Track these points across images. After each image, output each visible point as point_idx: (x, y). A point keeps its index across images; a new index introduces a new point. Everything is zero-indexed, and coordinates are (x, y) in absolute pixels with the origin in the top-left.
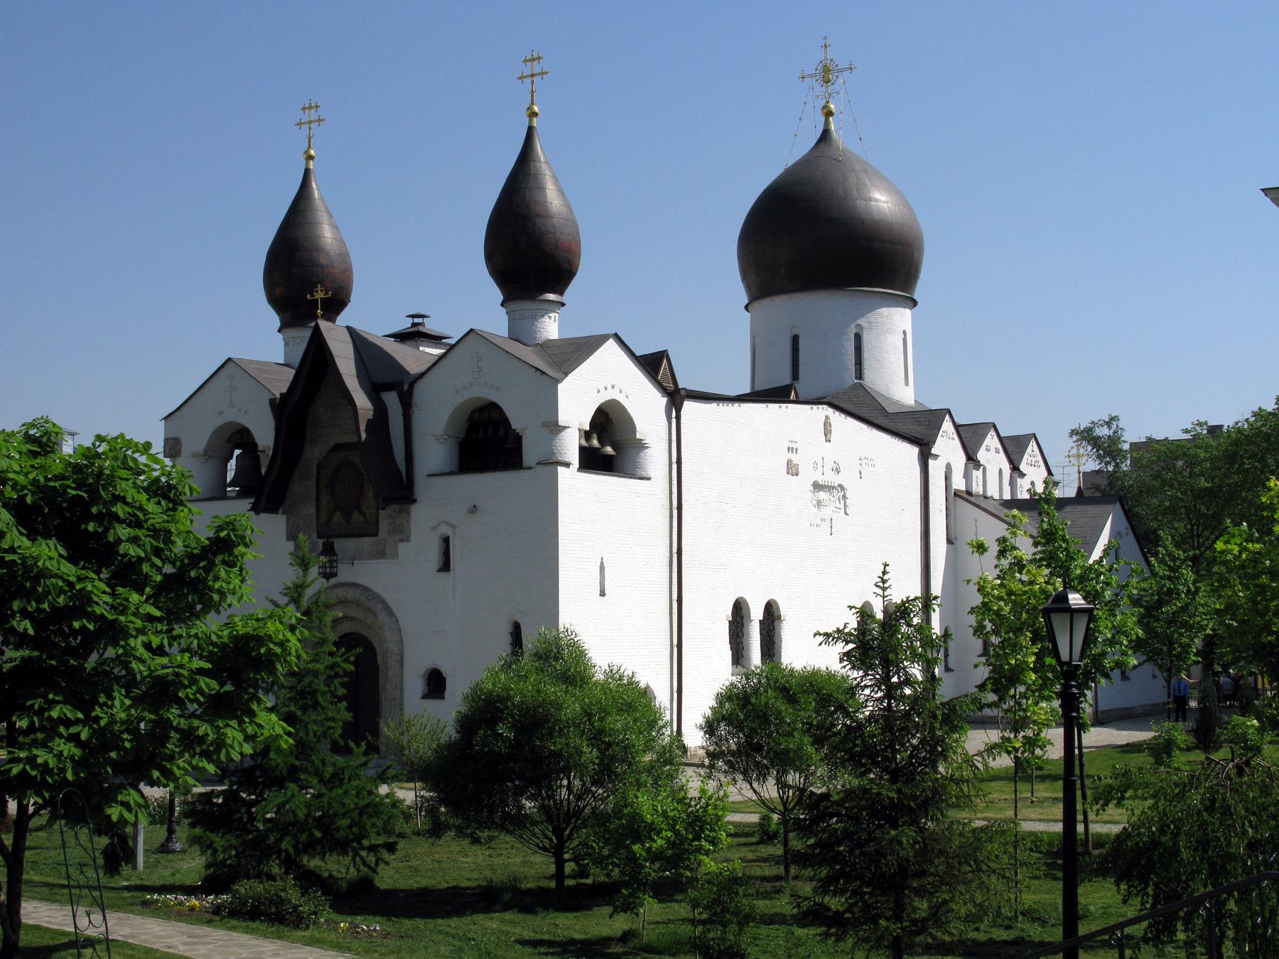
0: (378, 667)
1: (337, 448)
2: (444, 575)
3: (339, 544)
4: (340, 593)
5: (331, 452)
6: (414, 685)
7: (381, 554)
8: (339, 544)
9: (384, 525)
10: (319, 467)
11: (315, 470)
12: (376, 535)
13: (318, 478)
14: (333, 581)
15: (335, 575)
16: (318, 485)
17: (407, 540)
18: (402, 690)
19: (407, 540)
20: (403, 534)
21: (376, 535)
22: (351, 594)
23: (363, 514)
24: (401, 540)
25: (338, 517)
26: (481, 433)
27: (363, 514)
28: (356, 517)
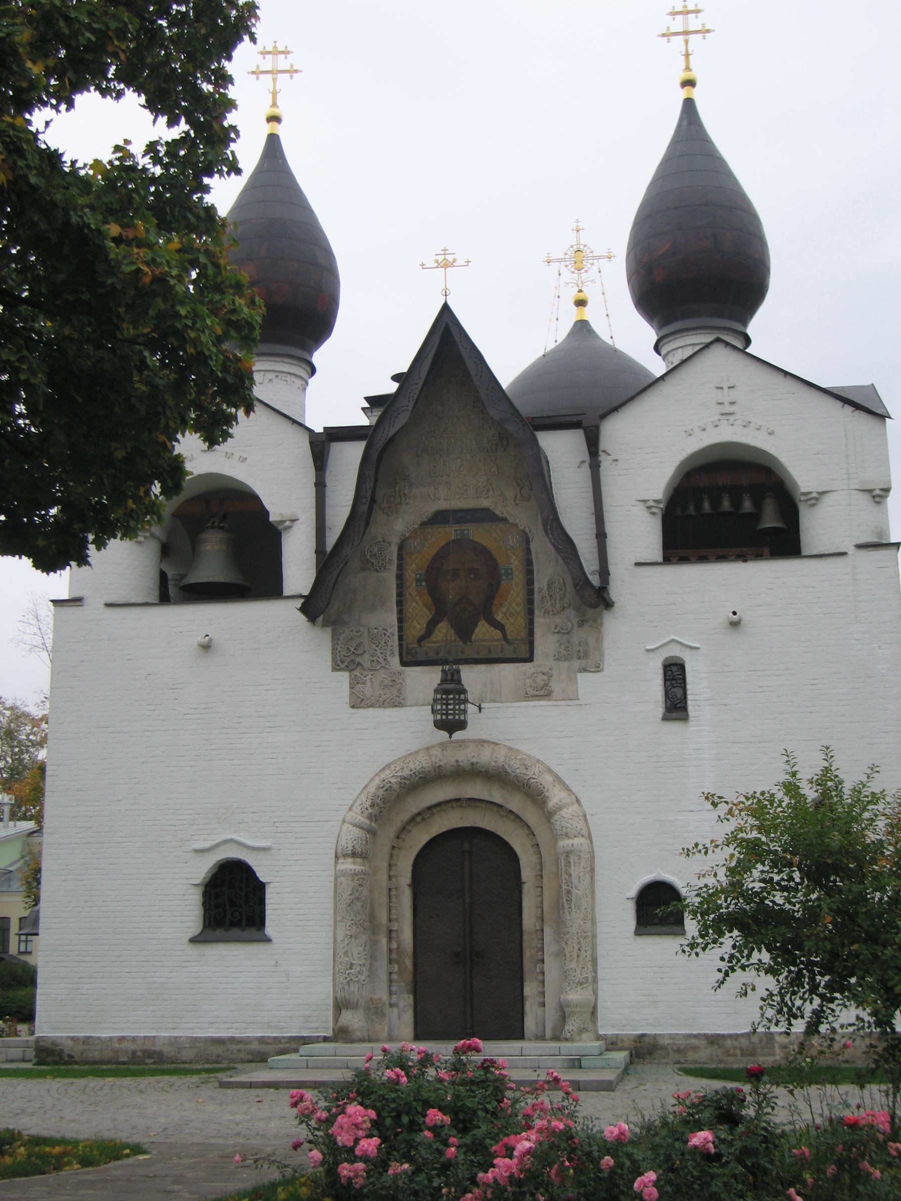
0: (518, 883)
1: (441, 518)
2: (675, 727)
3: (471, 676)
4: (465, 756)
5: (423, 524)
6: (616, 913)
7: (543, 693)
8: (471, 676)
9: (545, 643)
10: (401, 548)
11: (394, 550)
12: (530, 659)
13: (400, 567)
14: (458, 735)
15: (461, 725)
16: (400, 577)
17: (598, 669)
18: (594, 922)
19: (598, 669)
20: (585, 657)
21: (530, 659)
22: (485, 757)
23: (500, 626)
24: (585, 670)
25: (443, 631)
26: (707, 507)
27: (500, 626)
28: (483, 630)
